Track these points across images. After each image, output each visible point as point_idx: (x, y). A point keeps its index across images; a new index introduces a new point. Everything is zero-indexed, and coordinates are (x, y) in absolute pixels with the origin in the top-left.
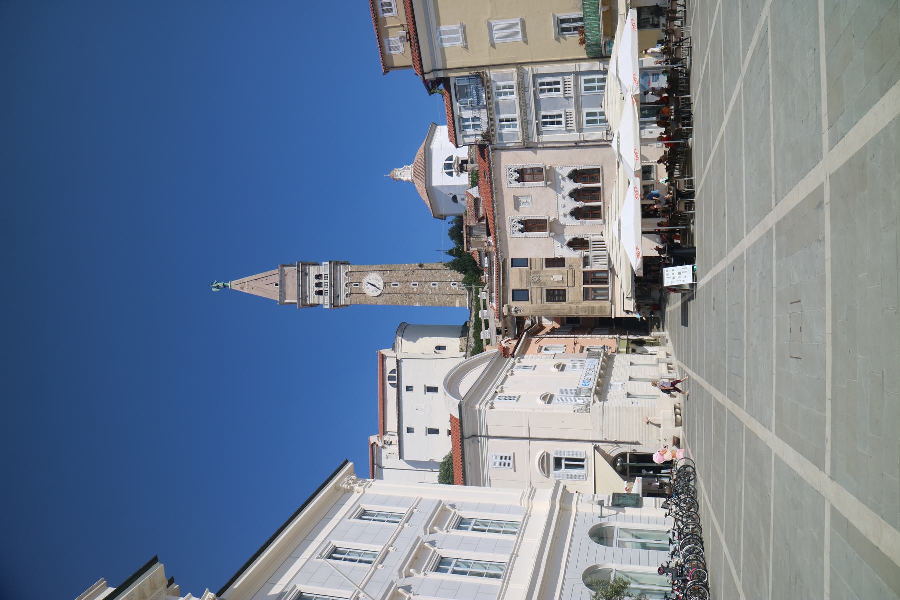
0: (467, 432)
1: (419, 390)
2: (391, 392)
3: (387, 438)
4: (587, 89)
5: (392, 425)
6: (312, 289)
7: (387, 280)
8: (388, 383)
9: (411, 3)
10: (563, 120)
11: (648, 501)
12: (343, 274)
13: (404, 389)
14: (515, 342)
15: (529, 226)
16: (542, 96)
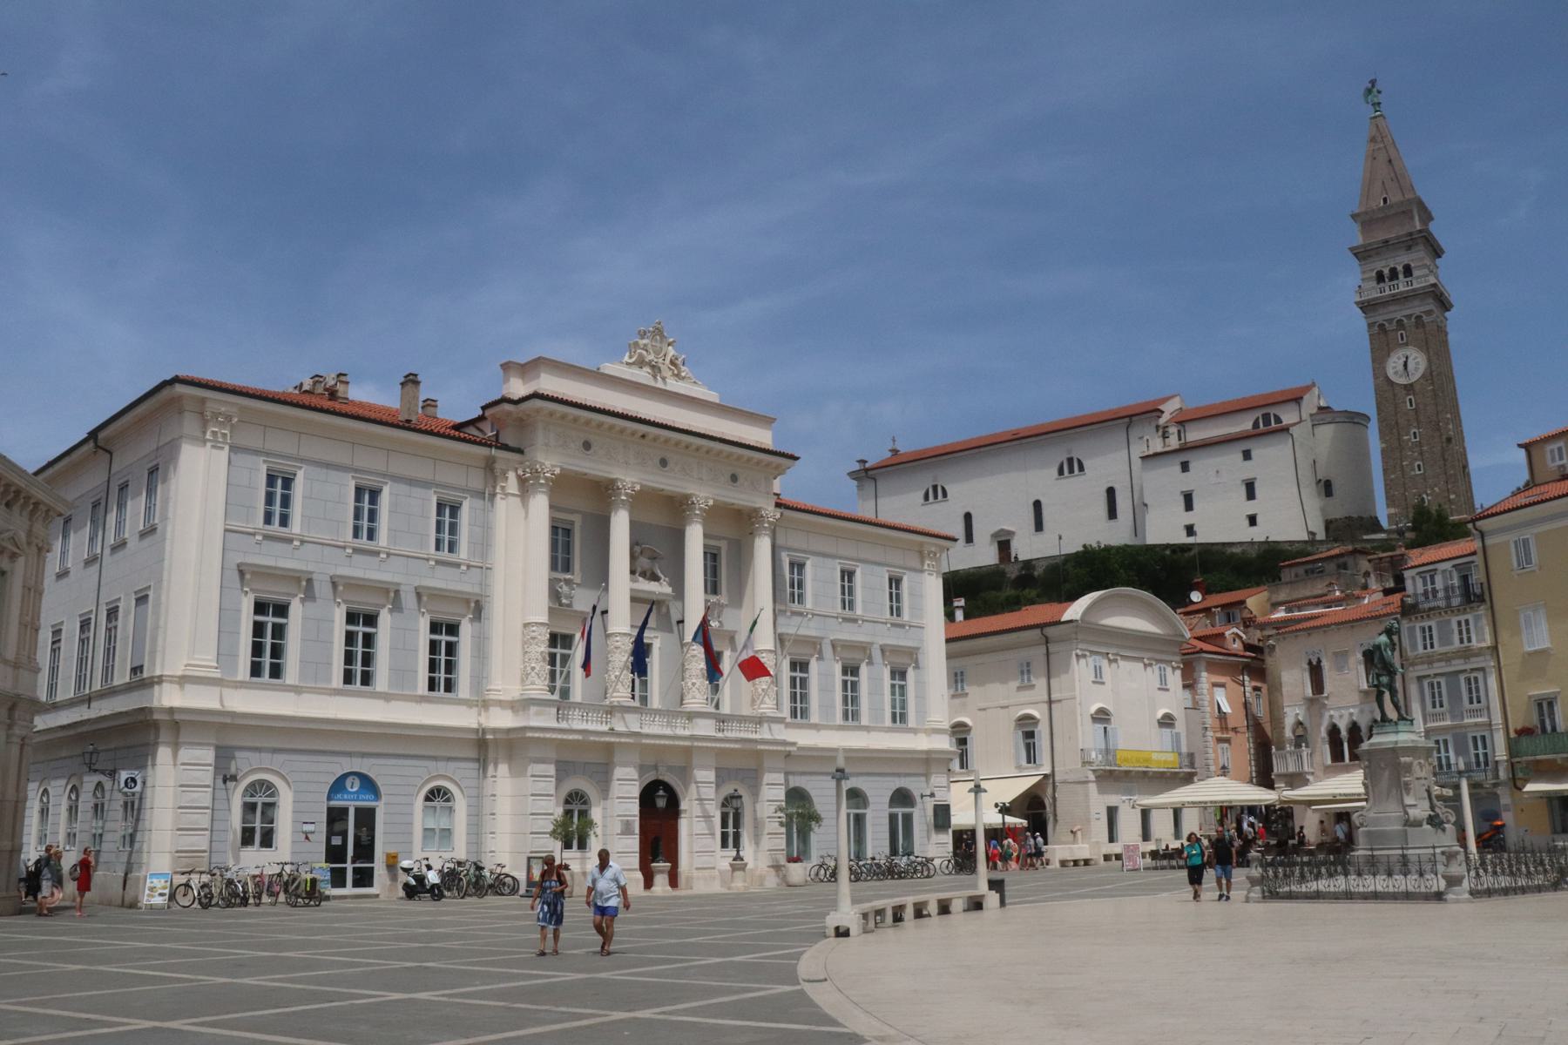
0: (1050, 631)
1: (1248, 470)
2: (1245, 424)
3: (1173, 430)
4: (1475, 738)
5: (1195, 434)
6: (1384, 265)
7: (1417, 388)
8: (1259, 413)
9: (1564, 496)
10: (1438, 709)
11: (948, 838)
12: (1417, 311)
13: (1245, 445)
14: (1237, 646)
15: (1316, 672)
16: (1462, 678)
